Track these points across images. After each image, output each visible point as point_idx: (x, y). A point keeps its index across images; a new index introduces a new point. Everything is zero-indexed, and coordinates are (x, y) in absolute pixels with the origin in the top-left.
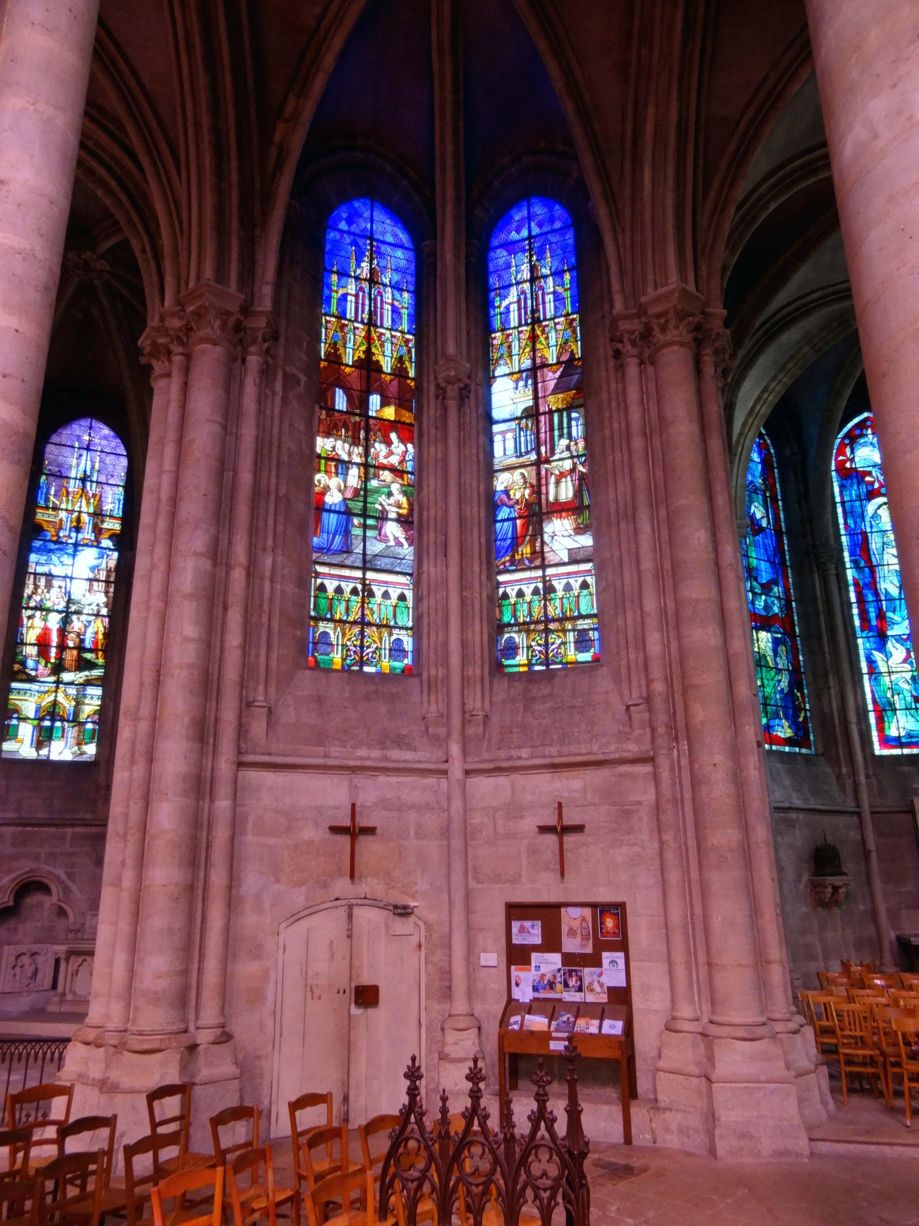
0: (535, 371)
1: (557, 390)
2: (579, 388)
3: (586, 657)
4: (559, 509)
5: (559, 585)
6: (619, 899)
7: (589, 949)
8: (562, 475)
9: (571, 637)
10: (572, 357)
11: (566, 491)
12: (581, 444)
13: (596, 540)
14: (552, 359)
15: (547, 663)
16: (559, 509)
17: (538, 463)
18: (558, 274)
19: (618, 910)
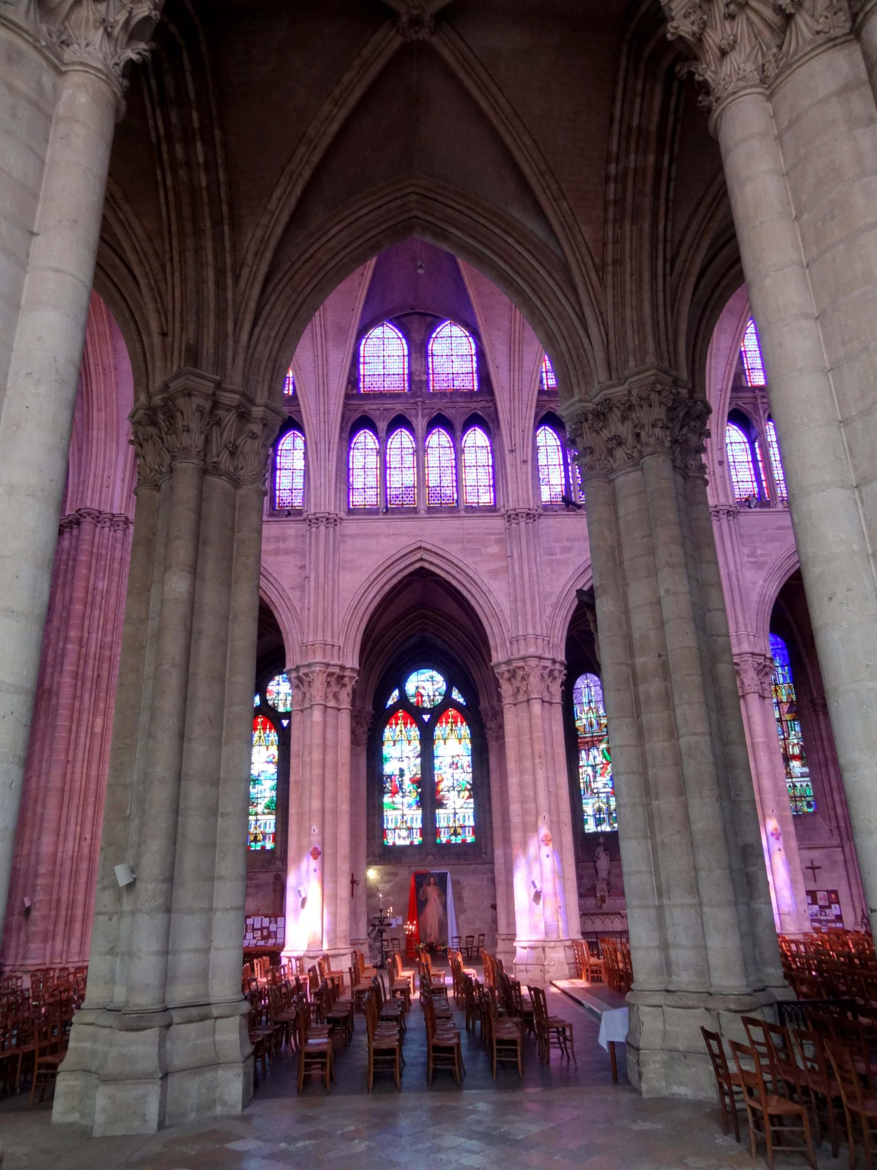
0: (779, 703)
1: (788, 712)
2: (796, 712)
3: (811, 810)
4: (794, 757)
5: (798, 785)
6: (836, 889)
7: (827, 904)
8: (794, 745)
9: (805, 803)
10: (792, 701)
11: (797, 751)
12: (800, 734)
13: (810, 768)
14: (785, 700)
15: (797, 811)
16: (794, 757)
17: (785, 739)
18: (782, 666)
19: (835, 892)
